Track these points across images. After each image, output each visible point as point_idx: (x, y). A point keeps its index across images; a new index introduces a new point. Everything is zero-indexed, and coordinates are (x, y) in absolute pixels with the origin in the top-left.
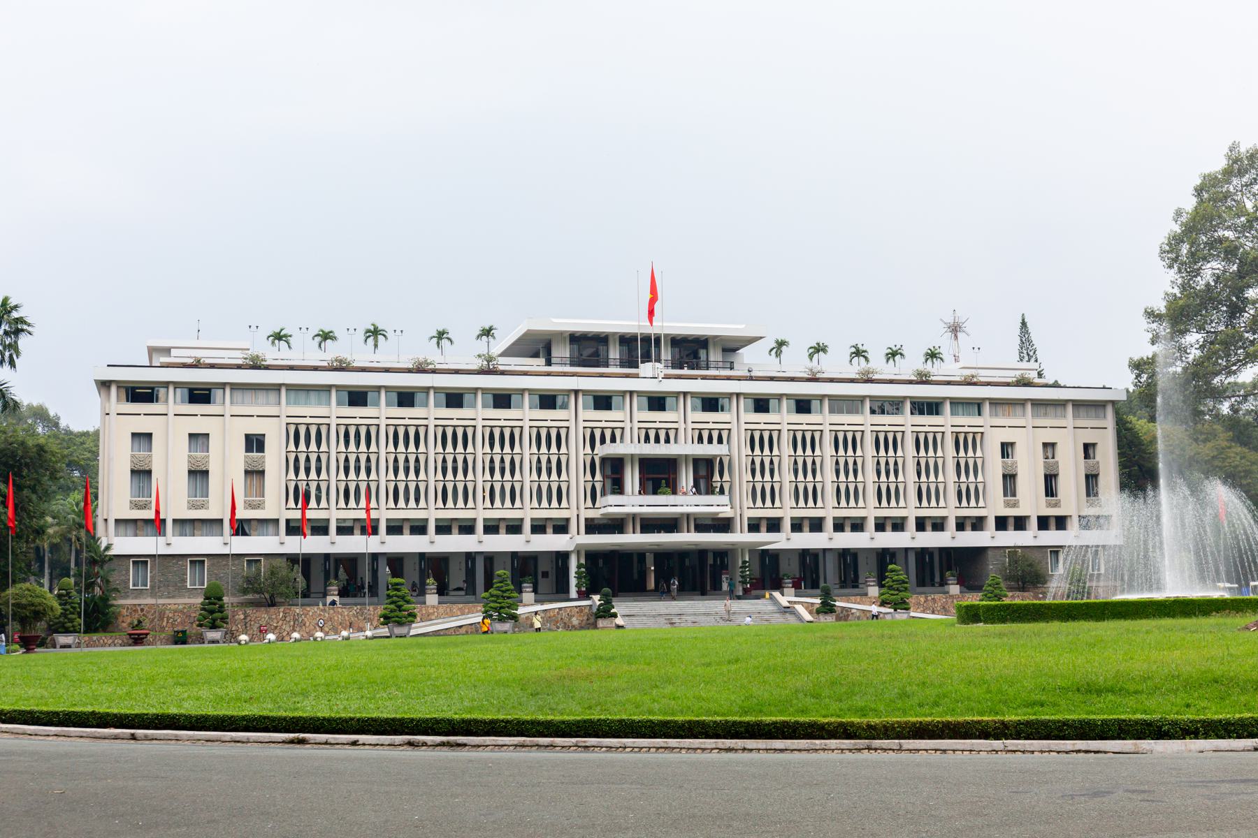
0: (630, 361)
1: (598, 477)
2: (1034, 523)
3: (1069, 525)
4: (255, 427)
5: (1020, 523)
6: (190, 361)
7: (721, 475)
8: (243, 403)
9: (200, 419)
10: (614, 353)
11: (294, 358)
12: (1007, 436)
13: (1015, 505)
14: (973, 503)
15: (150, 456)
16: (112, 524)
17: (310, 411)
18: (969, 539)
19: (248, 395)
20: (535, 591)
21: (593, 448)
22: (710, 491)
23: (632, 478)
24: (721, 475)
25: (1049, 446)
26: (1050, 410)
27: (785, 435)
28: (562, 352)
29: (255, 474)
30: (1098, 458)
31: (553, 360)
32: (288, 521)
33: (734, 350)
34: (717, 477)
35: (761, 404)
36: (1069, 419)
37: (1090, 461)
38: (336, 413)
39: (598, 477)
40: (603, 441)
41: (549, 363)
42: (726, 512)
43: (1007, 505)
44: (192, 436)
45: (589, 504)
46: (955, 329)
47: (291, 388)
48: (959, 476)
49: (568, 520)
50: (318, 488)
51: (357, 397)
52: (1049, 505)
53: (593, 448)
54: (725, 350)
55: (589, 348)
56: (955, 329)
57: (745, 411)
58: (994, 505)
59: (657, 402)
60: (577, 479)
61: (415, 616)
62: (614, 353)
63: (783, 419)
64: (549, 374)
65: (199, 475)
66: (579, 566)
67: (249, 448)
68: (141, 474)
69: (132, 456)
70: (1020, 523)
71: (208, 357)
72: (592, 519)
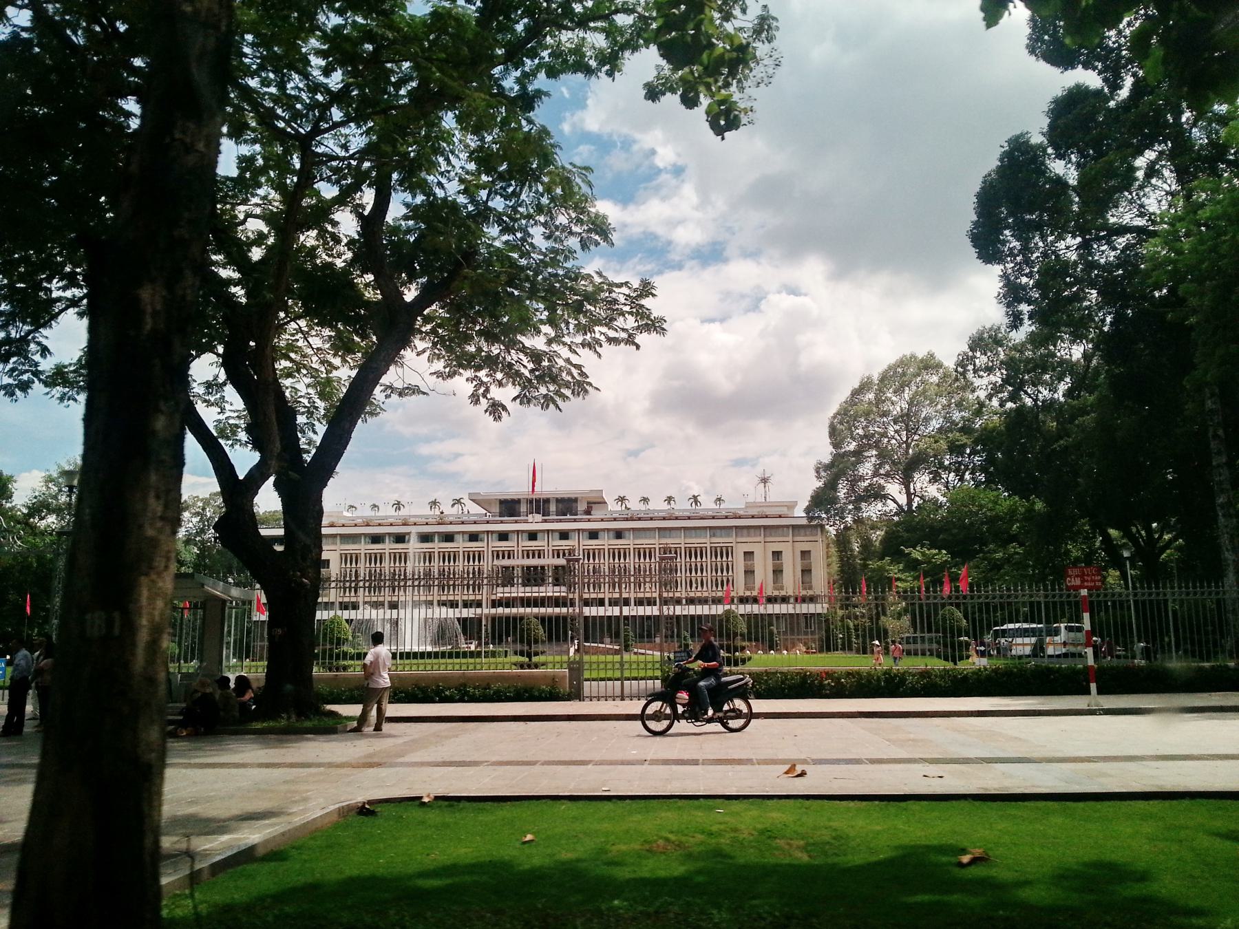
10: (523, 508)
12: (748, 548)
17: (351, 548)
25: (777, 555)
35: (594, 535)
38: (363, 548)
51: (377, 539)
52: (775, 589)
55: (509, 507)
58: (740, 590)
59: (533, 536)
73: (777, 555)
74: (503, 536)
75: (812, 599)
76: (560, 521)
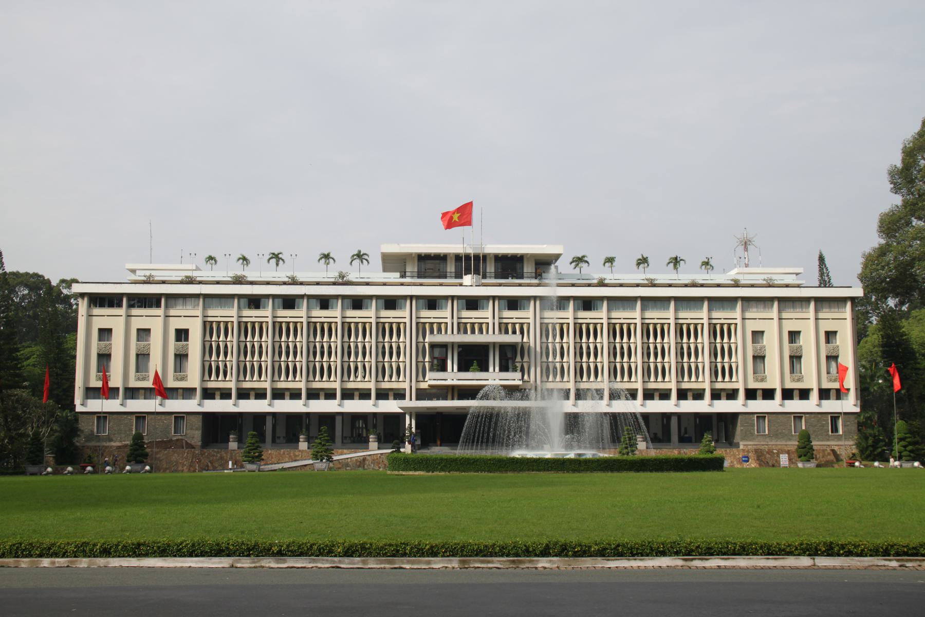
0: (459, 276)
1: (427, 359)
2: (778, 394)
3: (811, 398)
5: (768, 394)
7: (522, 357)
9: (145, 318)
10: (451, 268)
11: (220, 275)
13: (763, 380)
14: (727, 378)
17: (217, 313)
18: (724, 406)
21: (424, 338)
26: (798, 304)
28: (411, 268)
29: (181, 357)
30: (838, 343)
31: (408, 274)
34: (518, 359)
40: (432, 332)
41: (403, 276)
46: (746, 244)
51: (255, 302)
55: (431, 265)
56: (746, 244)
59: (473, 303)
62: (451, 268)
64: (402, 284)
65: (143, 357)
66: (410, 424)
68: (104, 358)
70: (768, 394)
71: (159, 276)
73: (794, 336)
74: (432, 303)
75: (840, 394)
76: (500, 285)
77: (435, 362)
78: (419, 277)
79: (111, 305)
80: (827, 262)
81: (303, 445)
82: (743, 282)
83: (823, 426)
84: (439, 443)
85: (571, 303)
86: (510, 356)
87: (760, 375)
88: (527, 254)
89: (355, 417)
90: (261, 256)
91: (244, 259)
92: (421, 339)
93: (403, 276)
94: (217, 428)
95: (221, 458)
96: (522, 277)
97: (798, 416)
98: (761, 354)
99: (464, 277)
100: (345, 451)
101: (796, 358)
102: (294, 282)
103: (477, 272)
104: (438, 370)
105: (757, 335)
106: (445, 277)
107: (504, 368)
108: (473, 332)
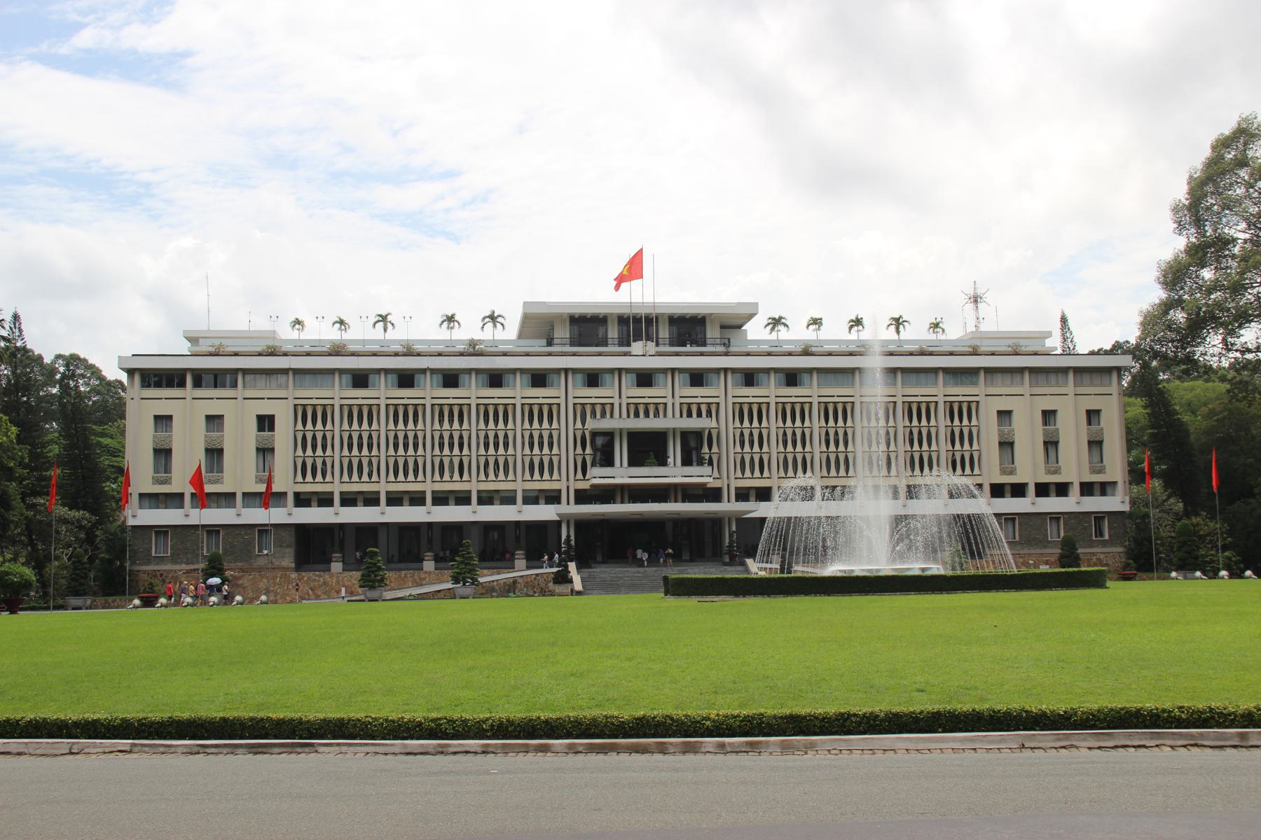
2: (1031, 490)
3: (1071, 493)
4: (266, 409)
6: (212, 350)
7: (710, 447)
8: (255, 387)
15: (171, 436)
16: (135, 499)
17: (314, 394)
19: (261, 380)
20: (529, 557)
21: (583, 423)
22: (700, 463)
23: (621, 452)
24: (710, 447)
25: (1048, 416)
26: (1053, 377)
27: (899, 406)
28: (562, 333)
29: (265, 452)
30: (1102, 424)
31: (556, 341)
32: (297, 495)
33: (740, 327)
34: (705, 449)
35: (749, 377)
36: (1070, 386)
37: (1093, 427)
38: (339, 394)
39: (588, 450)
41: (550, 344)
42: (711, 482)
43: (1004, 472)
44: (209, 418)
45: (580, 475)
46: (976, 300)
47: (297, 372)
48: (953, 444)
49: (560, 491)
50: (324, 463)
51: (360, 379)
52: (1049, 472)
53: (583, 423)
54: (722, 327)
55: (587, 327)
56: (976, 300)
57: (574, 386)
59: (645, 378)
60: (566, 452)
61: (382, 580)
62: (613, 332)
63: (771, 392)
64: (550, 354)
65: (215, 454)
66: (568, 536)
67: (261, 428)
68: (163, 454)
69: (154, 437)
70: (1018, 490)
72: (585, 490)
73: (1048, 416)
74: (593, 378)
75: (1105, 488)
76: (677, 354)
77: (599, 454)
78: (572, 345)
79: (170, 385)
80: (1071, 323)
81: (429, 565)
82: (983, 349)
83: (1085, 528)
84: (599, 558)
85: (772, 375)
86: (694, 447)
87: (1053, 465)
88: (711, 315)
89: (488, 527)
90: (364, 318)
91: (342, 322)
92: (579, 425)
93: (550, 344)
94: (313, 546)
95: (325, 583)
96: (704, 344)
97: (1055, 517)
98: (1054, 439)
99: (633, 344)
100: (486, 571)
101: (1051, 444)
102: (409, 353)
103: (649, 338)
104: (602, 466)
105: (1004, 415)
106: (604, 343)
107: (687, 462)
108: (647, 415)
